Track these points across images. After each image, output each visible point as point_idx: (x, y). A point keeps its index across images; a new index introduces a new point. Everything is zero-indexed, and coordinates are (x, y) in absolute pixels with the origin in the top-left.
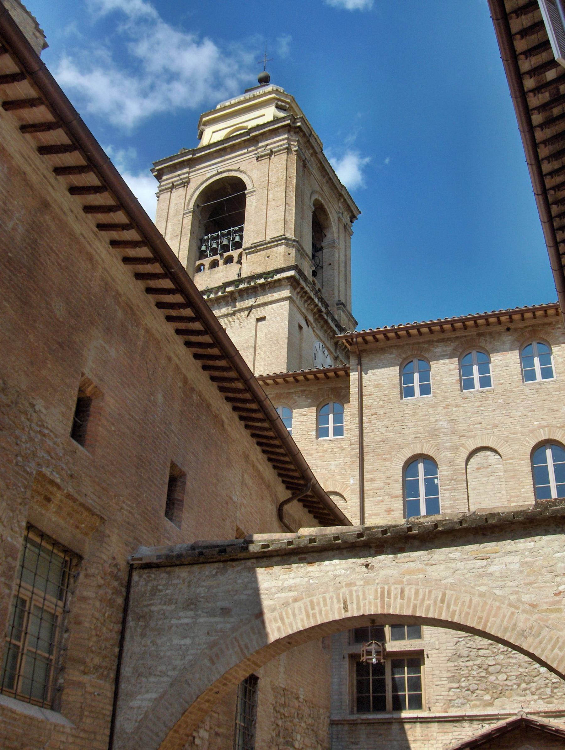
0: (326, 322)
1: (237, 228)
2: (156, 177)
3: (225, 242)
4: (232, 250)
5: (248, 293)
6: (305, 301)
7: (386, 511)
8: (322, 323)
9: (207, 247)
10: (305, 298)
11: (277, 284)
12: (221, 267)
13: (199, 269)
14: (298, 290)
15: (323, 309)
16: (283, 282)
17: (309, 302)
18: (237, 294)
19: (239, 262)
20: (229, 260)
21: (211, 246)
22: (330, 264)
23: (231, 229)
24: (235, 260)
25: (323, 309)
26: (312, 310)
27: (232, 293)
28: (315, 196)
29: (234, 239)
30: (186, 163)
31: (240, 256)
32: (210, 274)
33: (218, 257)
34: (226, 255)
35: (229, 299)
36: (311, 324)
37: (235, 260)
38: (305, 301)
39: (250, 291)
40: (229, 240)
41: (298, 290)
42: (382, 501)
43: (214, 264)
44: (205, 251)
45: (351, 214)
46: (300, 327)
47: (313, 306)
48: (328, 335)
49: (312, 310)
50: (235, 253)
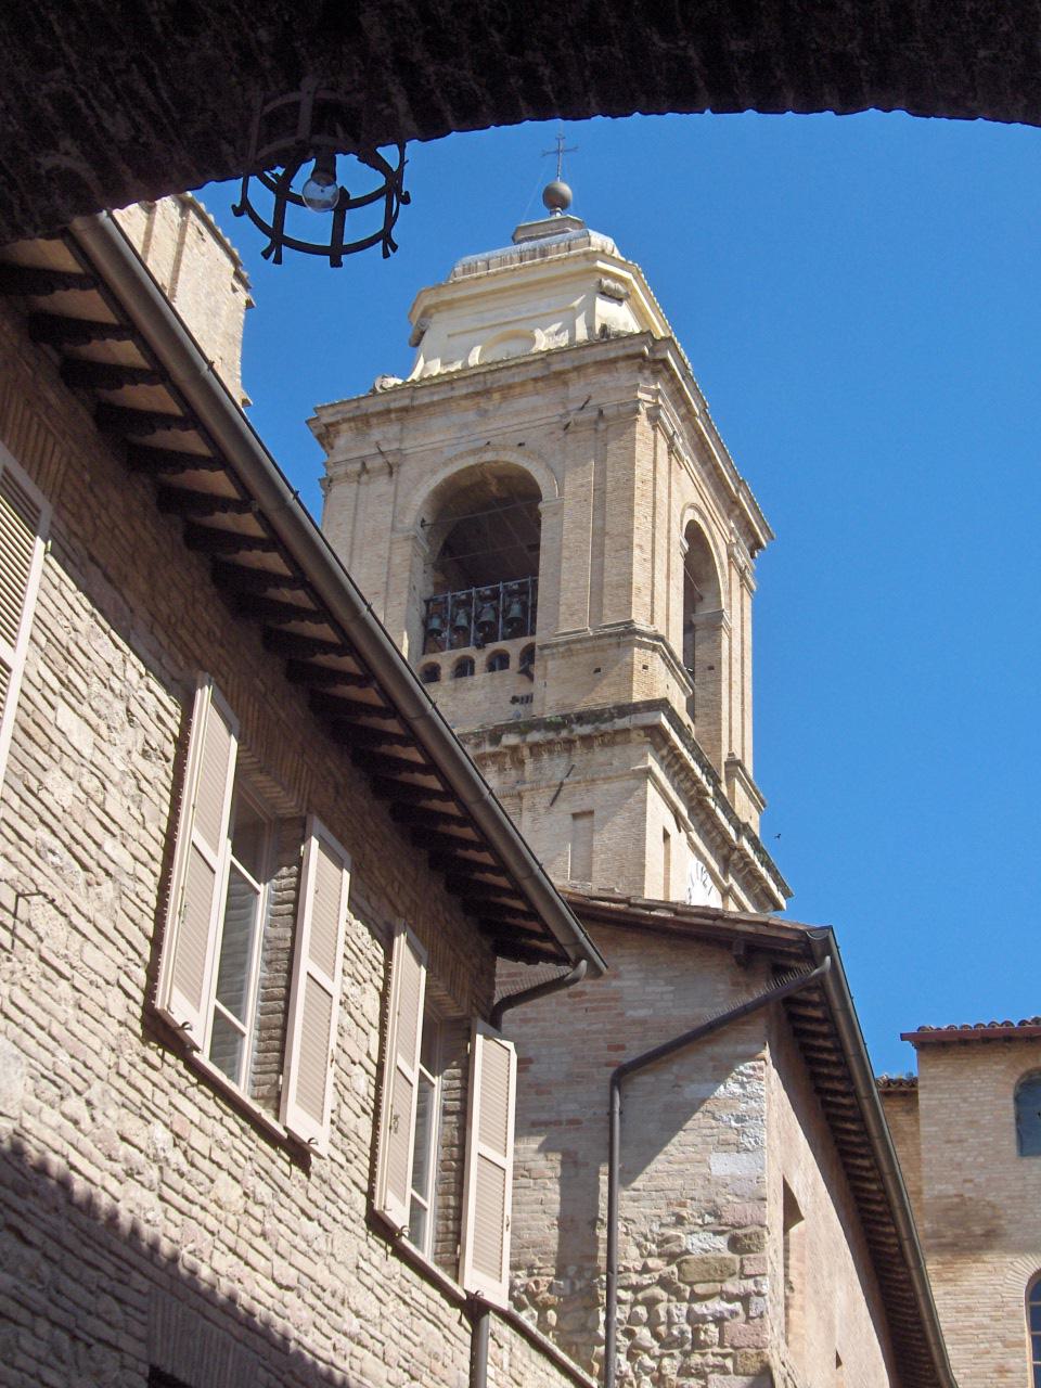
0: (711, 815)
1: (514, 585)
2: (320, 437)
3: (488, 616)
4: (504, 638)
5: (551, 752)
6: (676, 774)
7: (995, 1371)
8: (702, 816)
9: (444, 623)
10: (676, 768)
11: (619, 738)
12: (480, 676)
13: (432, 674)
14: (664, 752)
15: (710, 790)
16: (634, 735)
17: (682, 776)
18: (526, 752)
19: (527, 672)
20: (499, 662)
21: (453, 620)
22: (711, 668)
23: (501, 585)
24: (514, 663)
25: (710, 790)
26: (686, 792)
27: (514, 749)
28: (691, 515)
29: (507, 610)
30: (393, 416)
31: (528, 655)
32: (455, 690)
33: (470, 651)
34: (492, 647)
35: (508, 760)
36: (686, 824)
37: (514, 663)
38: (676, 774)
39: (558, 748)
40: (496, 609)
41: (664, 752)
42: (988, 1353)
43: (464, 668)
44: (439, 633)
45: (752, 541)
46: (666, 836)
47: (688, 784)
48: (712, 840)
49: (686, 792)
50: (513, 648)
